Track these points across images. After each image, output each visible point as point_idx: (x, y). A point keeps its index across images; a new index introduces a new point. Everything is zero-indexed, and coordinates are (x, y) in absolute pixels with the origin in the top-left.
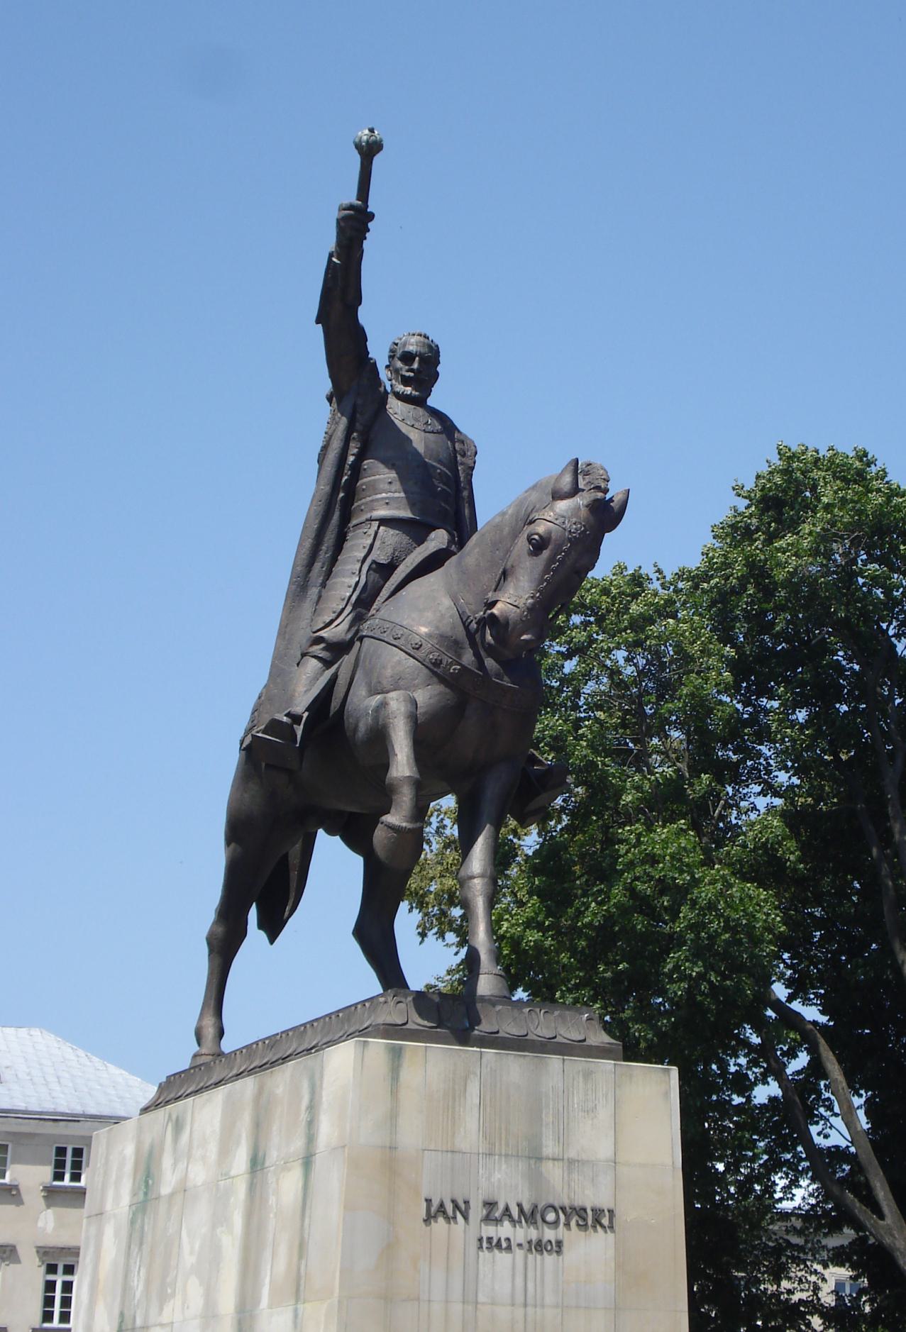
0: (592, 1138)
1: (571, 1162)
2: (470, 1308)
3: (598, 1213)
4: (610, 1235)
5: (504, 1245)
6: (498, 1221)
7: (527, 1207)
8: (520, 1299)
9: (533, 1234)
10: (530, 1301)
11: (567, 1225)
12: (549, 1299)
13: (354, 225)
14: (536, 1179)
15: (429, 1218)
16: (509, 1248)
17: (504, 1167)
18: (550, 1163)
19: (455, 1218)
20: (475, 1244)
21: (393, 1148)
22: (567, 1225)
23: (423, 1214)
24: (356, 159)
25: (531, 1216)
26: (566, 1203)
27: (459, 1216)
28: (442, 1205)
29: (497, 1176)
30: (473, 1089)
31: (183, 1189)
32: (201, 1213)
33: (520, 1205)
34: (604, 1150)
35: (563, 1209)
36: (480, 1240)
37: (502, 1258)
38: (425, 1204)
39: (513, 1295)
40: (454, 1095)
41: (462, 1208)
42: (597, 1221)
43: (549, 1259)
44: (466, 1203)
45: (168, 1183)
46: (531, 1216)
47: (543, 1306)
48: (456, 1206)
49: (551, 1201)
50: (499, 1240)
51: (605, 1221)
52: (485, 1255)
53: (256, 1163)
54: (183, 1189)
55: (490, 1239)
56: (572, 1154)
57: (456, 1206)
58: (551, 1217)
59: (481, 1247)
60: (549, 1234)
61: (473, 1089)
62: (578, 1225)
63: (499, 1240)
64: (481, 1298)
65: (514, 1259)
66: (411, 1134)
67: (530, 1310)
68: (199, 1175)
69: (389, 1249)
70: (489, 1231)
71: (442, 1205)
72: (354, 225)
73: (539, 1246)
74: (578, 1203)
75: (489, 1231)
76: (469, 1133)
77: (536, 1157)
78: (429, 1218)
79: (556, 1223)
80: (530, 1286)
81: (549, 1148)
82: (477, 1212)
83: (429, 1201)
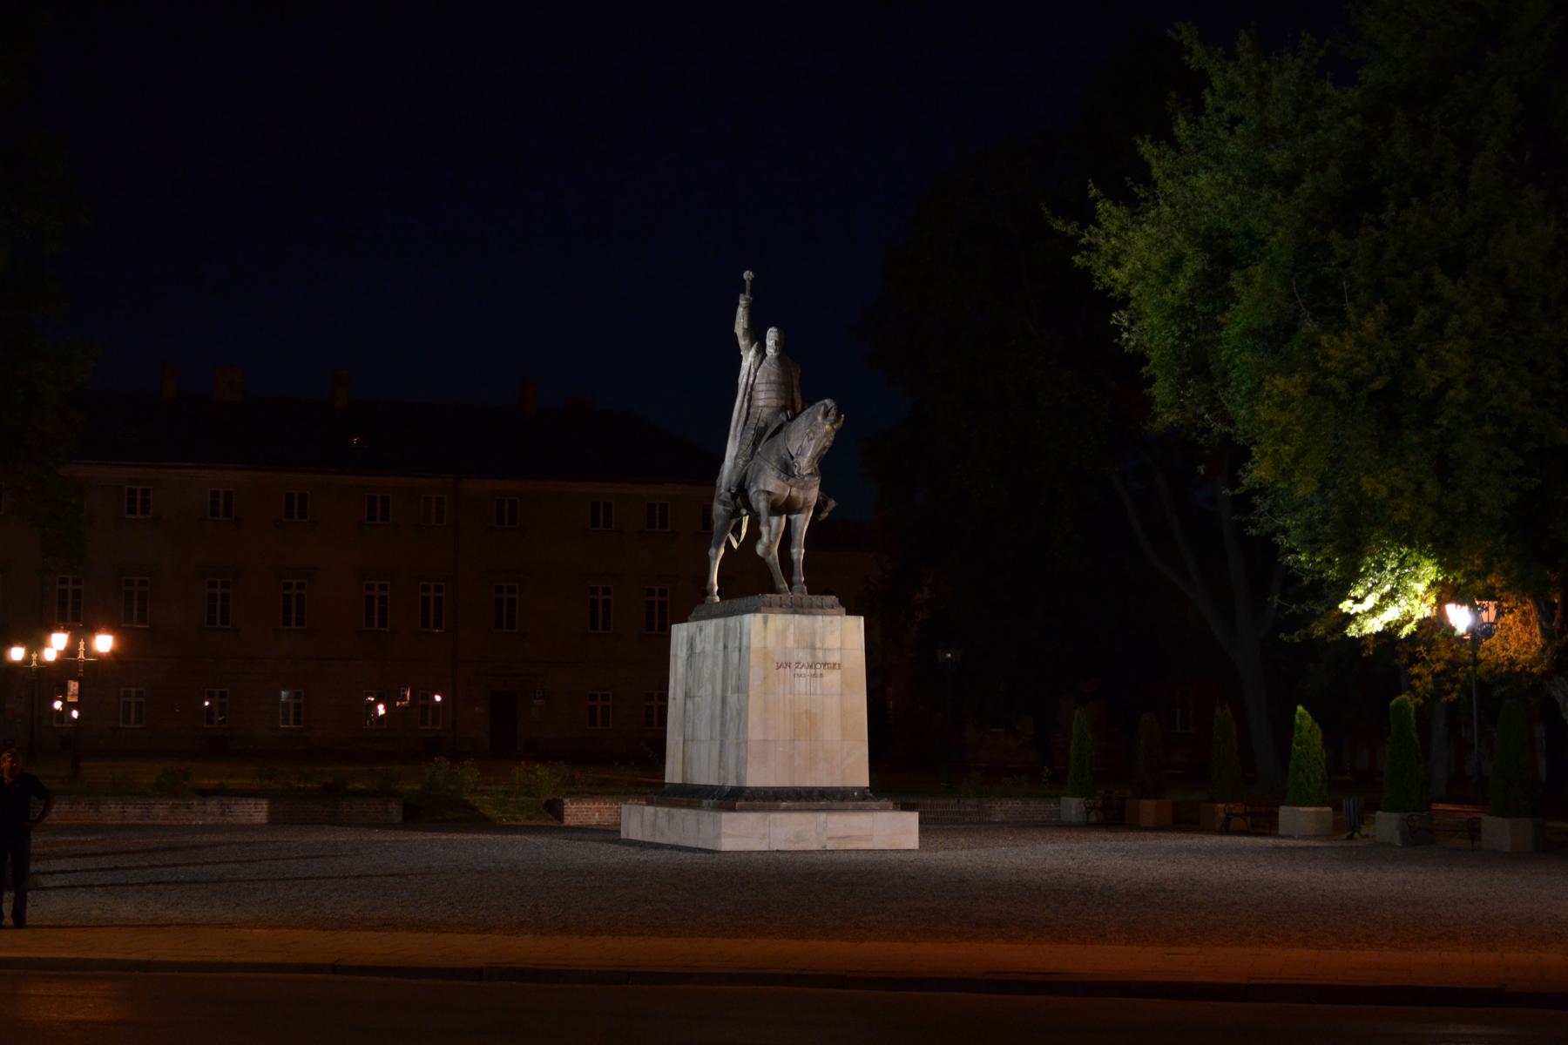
0: (833, 641)
31: (703, 651)
32: (709, 661)
34: (838, 645)
37: (803, 680)
45: (698, 649)
53: (725, 647)
54: (703, 651)
66: (771, 643)
68: (708, 648)
76: (790, 642)
77: (813, 648)
81: (818, 645)
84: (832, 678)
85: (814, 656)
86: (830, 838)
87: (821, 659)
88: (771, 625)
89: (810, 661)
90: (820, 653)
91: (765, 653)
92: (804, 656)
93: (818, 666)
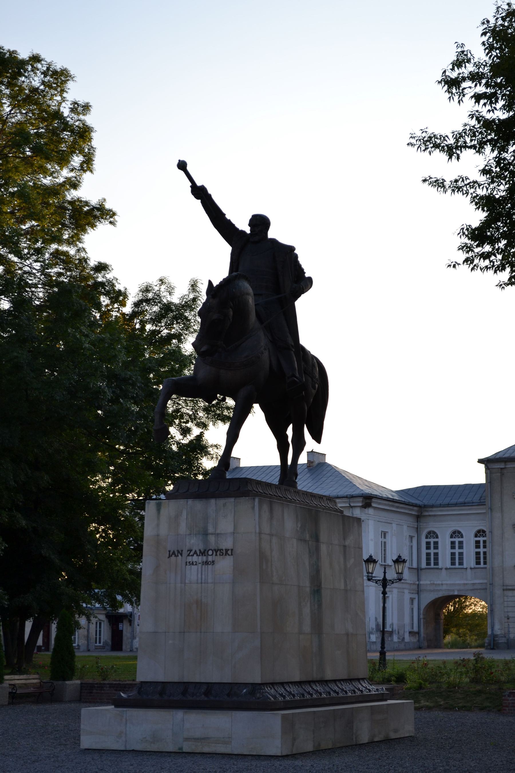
1: (218, 534)
2: (183, 585)
3: (227, 550)
4: (232, 557)
5: (195, 563)
6: (193, 555)
7: (202, 551)
8: (200, 581)
9: (204, 558)
10: (203, 581)
11: (216, 555)
12: (210, 581)
13: (200, 192)
14: (206, 542)
15: (170, 556)
16: (196, 564)
17: (195, 538)
18: (211, 536)
19: (178, 556)
20: (184, 564)
21: (158, 535)
22: (216, 555)
23: (168, 555)
24: (182, 173)
25: (203, 553)
26: (216, 548)
27: (179, 555)
28: (174, 552)
29: (192, 541)
30: (184, 513)
33: (200, 550)
34: (230, 529)
35: (215, 550)
36: (187, 562)
37: (194, 568)
38: (168, 553)
39: (197, 579)
40: (177, 517)
41: (180, 553)
42: (227, 553)
43: (210, 566)
44: (182, 551)
46: (203, 553)
47: (207, 583)
48: (178, 551)
49: (211, 548)
50: (193, 562)
51: (229, 552)
52: (188, 567)
55: (189, 562)
56: (218, 531)
57: (178, 551)
58: (210, 552)
59: (186, 565)
60: (210, 559)
61: (184, 513)
62: (220, 555)
63: (193, 562)
64: (187, 581)
65: (198, 569)
66: (164, 531)
67: (203, 584)
69: (157, 568)
70: (190, 559)
71: (174, 552)
72: (200, 192)
73: (207, 563)
74: (220, 548)
75: (190, 559)
76: (183, 528)
77: (206, 534)
78: (170, 556)
79: (212, 555)
80: (203, 576)
81: (211, 530)
82: (185, 553)
83: (170, 551)
84: (225, 564)
85: (206, 542)
86: (187, 739)
87: (213, 546)
88: (164, 511)
89: (201, 547)
90: (212, 539)
91: (158, 540)
92: (195, 543)
93: (209, 553)
